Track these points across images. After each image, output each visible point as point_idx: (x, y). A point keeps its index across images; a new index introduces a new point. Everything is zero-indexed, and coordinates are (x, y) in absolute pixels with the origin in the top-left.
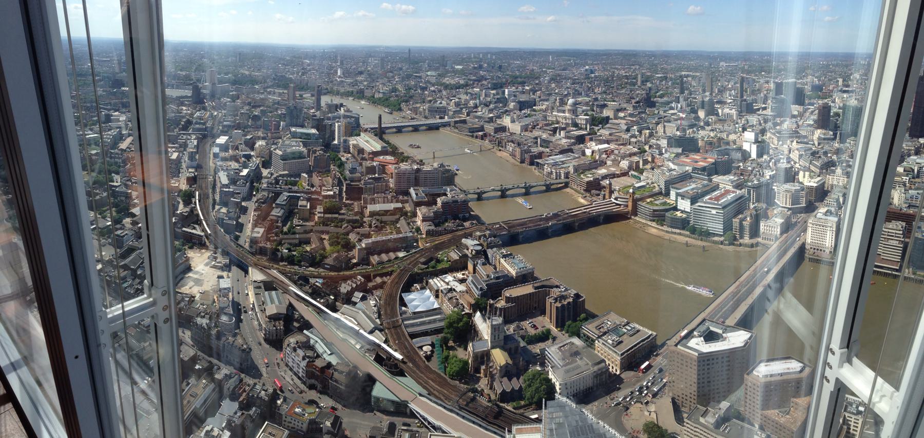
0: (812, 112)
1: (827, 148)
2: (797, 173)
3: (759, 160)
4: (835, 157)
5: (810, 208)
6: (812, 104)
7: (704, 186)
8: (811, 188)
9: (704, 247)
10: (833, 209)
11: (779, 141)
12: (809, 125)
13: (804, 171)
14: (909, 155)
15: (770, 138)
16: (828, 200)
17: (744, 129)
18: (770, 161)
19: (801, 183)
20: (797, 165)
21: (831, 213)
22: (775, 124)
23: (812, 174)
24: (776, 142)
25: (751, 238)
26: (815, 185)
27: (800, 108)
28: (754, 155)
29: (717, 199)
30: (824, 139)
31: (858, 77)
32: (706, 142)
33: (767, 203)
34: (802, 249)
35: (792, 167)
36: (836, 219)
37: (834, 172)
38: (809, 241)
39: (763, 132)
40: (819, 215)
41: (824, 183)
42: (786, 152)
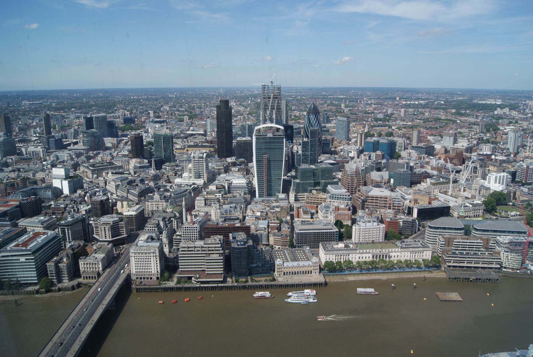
0: (126, 143)
1: (143, 175)
2: (115, 204)
3: (73, 196)
4: (152, 184)
5: (132, 238)
6: (126, 136)
7: (6, 233)
8: (130, 218)
9: (16, 301)
10: (154, 235)
11: (93, 174)
12: (124, 156)
13: (122, 201)
14: (220, 174)
15: (83, 172)
16: (149, 226)
17: (54, 165)
18: (85, 195)
19: (121, 214)
20: (114, 196)
21: (152, 239)
22: (89, 158)
23: (130, 203)
24: (91, 176)
25: (71, 279)
26: (134, 213)
27: (114, 140)
28: (66, 191)
29: (25, 244)
30: (141, 167)
31: (168, 109)
32: (6, 184)
33: (86, 241)
34: (128, 280)
35: (108, 199)
36: (158, 244)
37: (152, 198)
38: (133, 271)
39: (76, 167)
40: (140, 243)
41: (143, 211)
42: (102, 184)
